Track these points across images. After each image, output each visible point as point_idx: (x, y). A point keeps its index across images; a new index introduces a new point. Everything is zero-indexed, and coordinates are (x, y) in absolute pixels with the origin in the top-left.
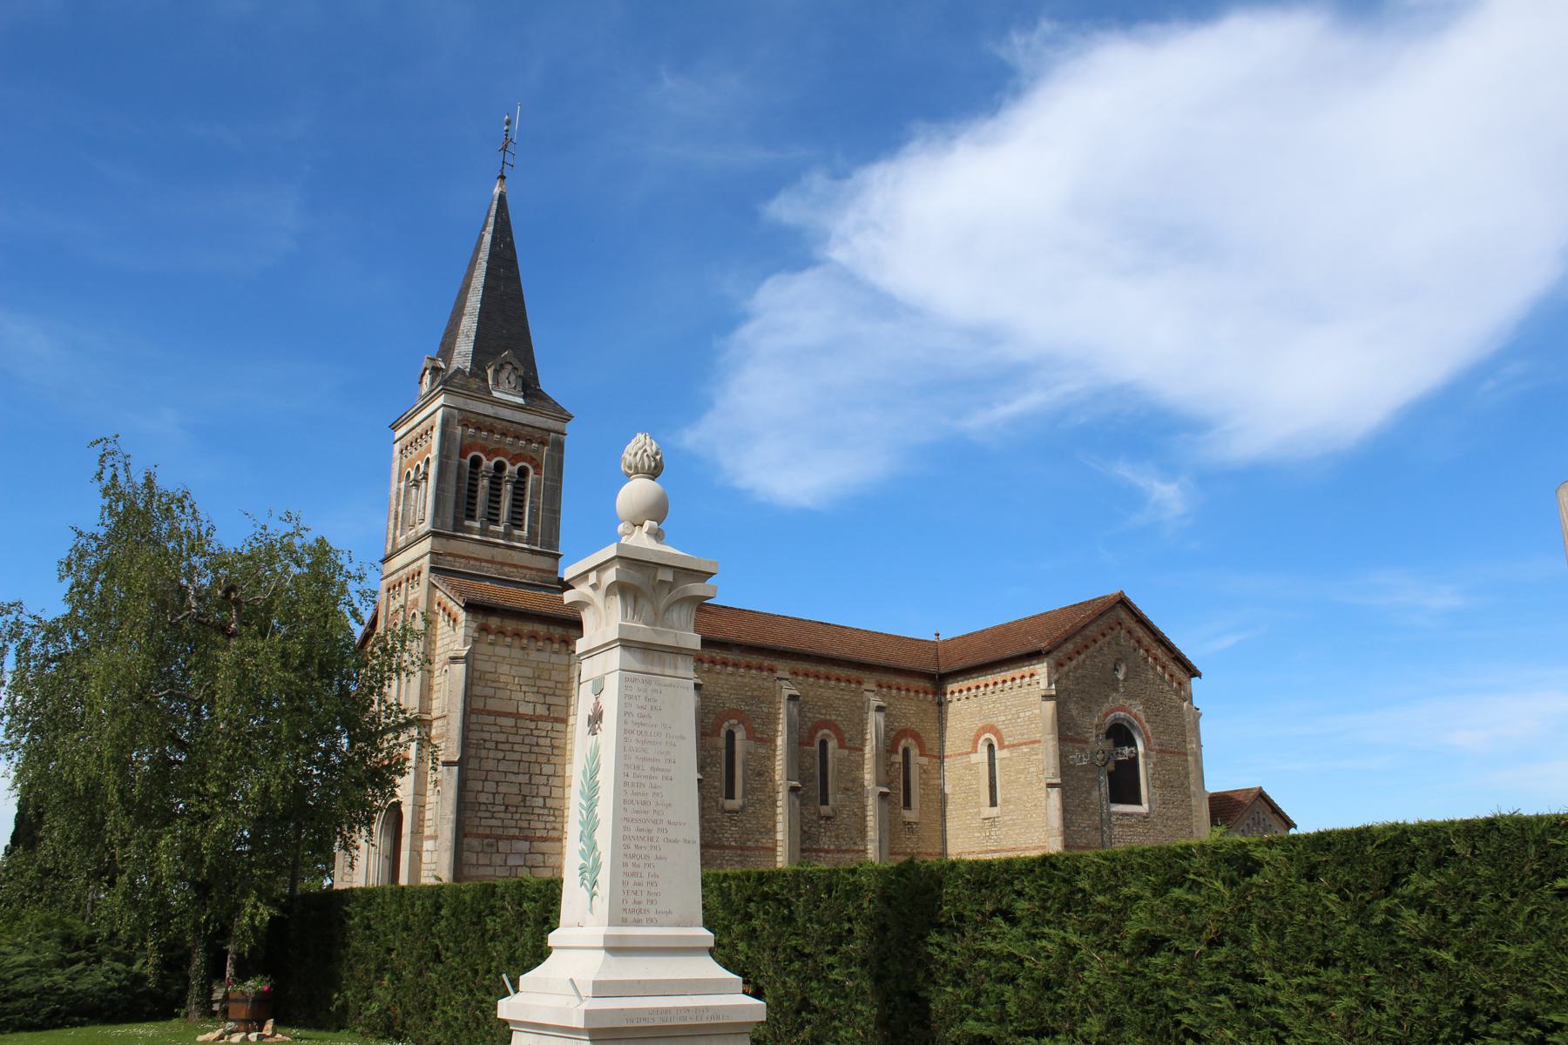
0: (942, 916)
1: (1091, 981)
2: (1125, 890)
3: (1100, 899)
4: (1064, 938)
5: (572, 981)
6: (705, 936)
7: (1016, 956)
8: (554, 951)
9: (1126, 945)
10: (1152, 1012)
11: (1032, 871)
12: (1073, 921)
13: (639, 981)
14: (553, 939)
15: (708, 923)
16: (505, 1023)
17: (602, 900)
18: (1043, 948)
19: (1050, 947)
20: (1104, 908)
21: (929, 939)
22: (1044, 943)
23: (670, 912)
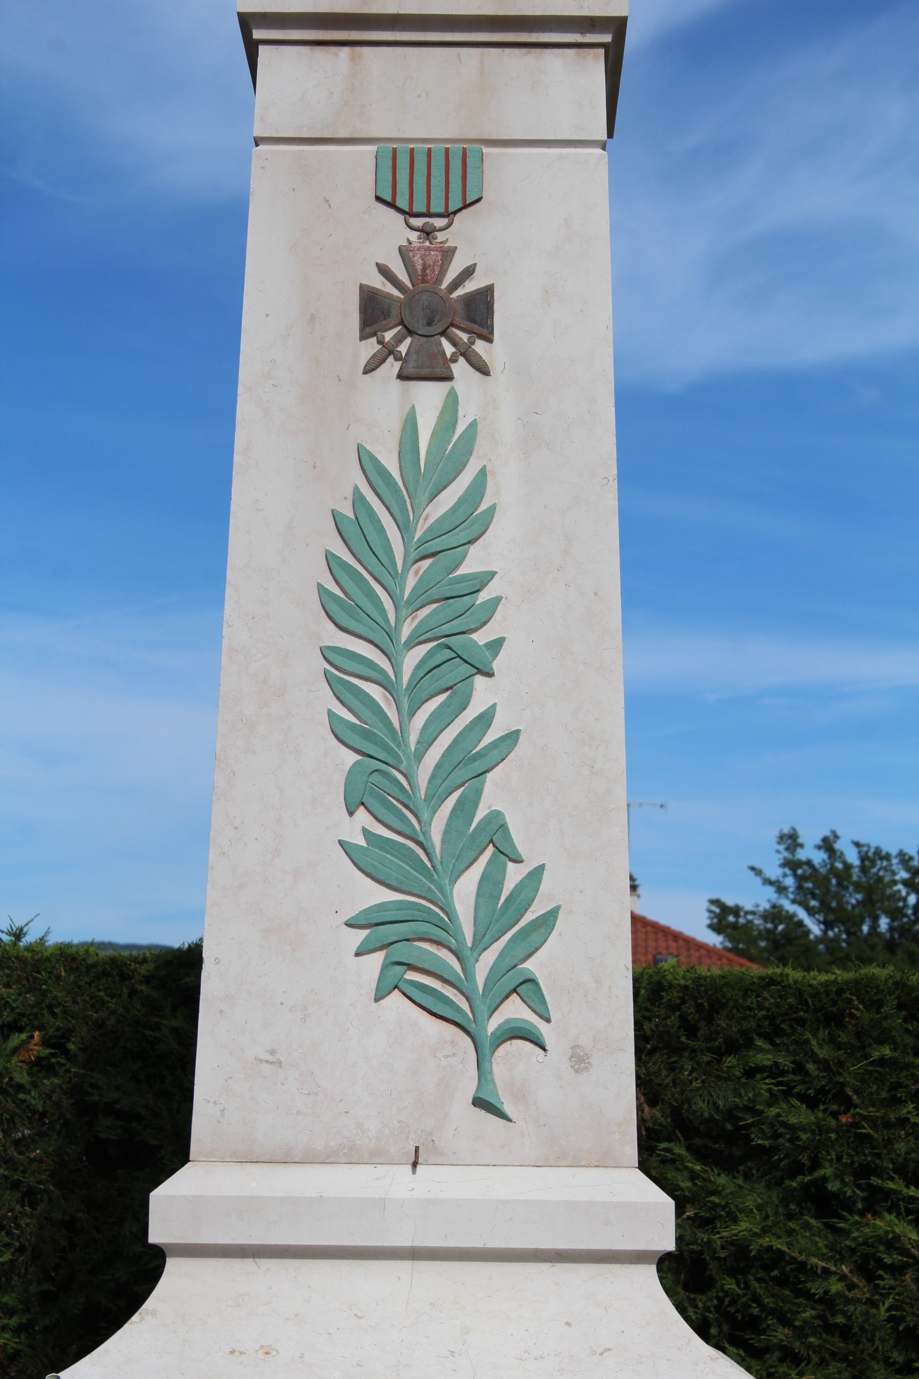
8: (172, 1265)
18: (892, 1243)
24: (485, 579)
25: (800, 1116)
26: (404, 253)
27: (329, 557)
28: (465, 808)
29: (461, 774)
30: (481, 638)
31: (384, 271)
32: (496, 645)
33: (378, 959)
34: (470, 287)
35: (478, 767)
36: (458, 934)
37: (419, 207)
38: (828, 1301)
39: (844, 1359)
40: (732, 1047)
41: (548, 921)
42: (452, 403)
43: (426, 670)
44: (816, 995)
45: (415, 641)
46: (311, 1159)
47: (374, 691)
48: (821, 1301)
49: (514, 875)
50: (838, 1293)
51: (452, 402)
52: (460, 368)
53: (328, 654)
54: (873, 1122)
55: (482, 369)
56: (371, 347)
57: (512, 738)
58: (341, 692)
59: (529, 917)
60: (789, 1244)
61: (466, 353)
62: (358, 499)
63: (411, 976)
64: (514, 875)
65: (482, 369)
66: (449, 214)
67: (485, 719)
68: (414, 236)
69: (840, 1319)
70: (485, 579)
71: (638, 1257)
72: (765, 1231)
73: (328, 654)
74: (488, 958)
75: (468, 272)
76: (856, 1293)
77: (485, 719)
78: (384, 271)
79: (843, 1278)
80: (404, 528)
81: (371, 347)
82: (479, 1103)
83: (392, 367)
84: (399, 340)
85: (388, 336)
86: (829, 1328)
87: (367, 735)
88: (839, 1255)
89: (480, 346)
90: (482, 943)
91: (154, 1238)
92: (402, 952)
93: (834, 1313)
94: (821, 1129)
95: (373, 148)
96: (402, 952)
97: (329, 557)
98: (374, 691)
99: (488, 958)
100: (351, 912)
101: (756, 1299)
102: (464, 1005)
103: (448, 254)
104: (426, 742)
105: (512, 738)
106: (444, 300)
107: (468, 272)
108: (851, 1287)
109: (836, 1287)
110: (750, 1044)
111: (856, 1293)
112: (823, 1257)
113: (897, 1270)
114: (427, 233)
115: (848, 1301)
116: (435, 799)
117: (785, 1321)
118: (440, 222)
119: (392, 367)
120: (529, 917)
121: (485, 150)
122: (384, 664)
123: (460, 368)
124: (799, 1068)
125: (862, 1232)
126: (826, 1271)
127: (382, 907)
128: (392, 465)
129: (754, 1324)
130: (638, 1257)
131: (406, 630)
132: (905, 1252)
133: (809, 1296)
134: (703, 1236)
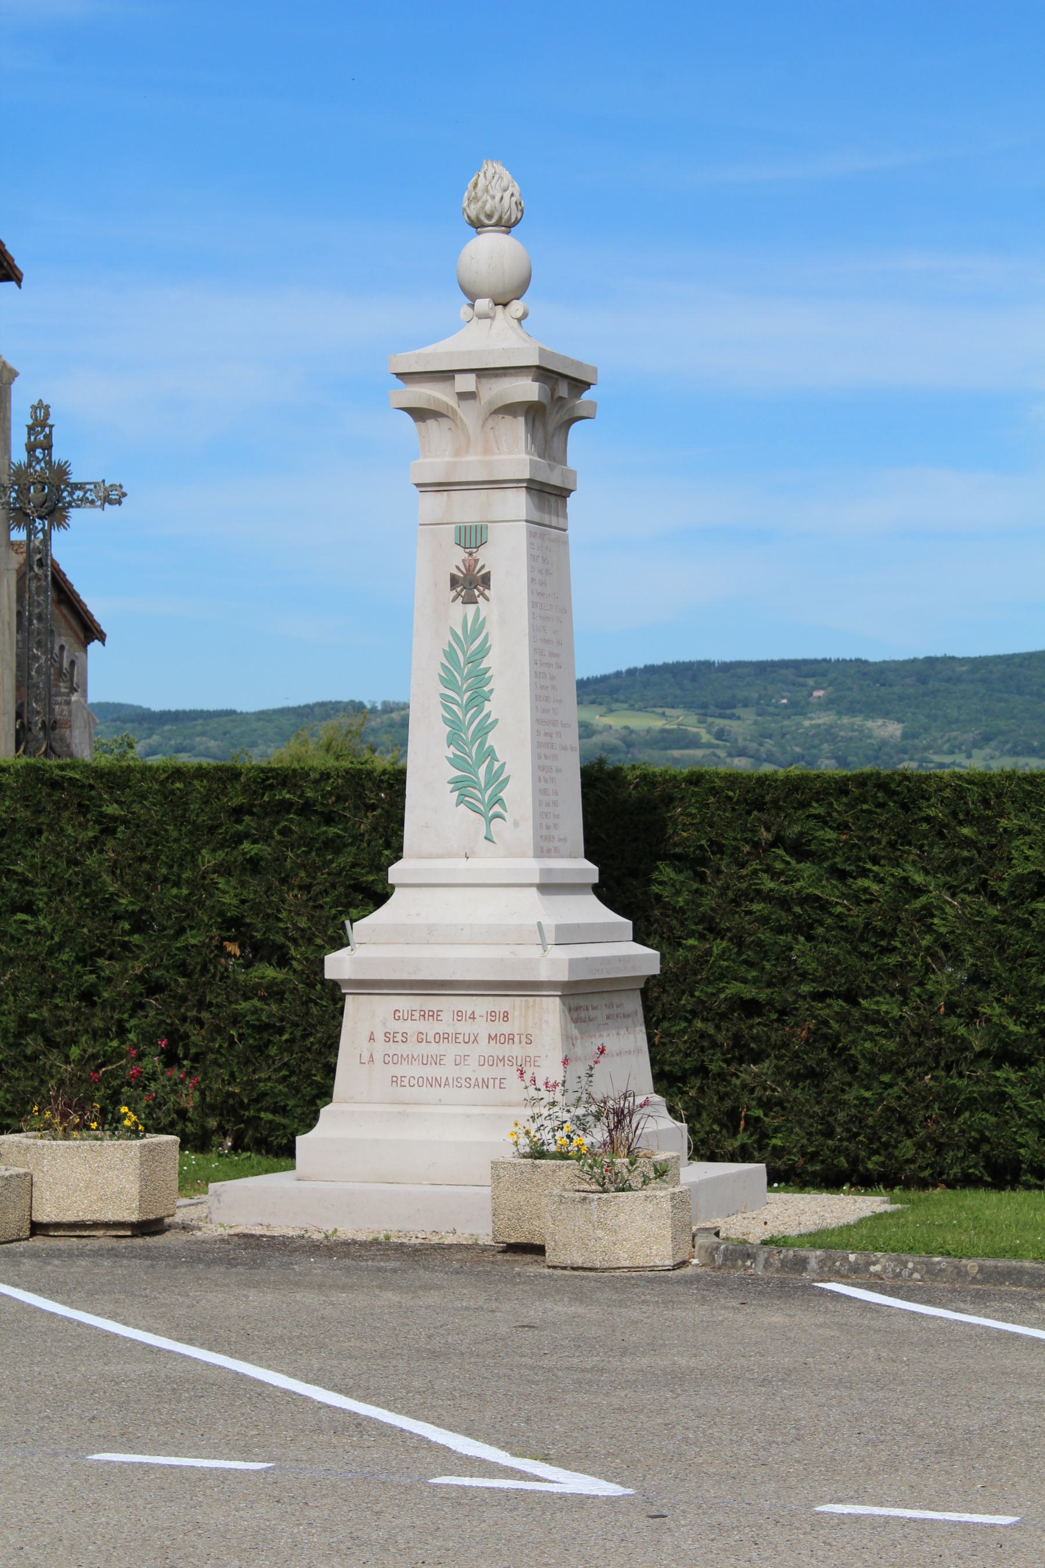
0: (675, 845)
1: (943, 930)
2: (1004, 822)
3: (966, 831)
4: (905, 879)
5: (539, 924)
6: (590, 871)
7: (818, 898)
8: (396, 889)
9: (1003, 889)
10: (1033, 965)
11: (846, 792)
12: (911, 857)
13: (578, 925)
14: (396, 873)
15: (590, 855)
16: (335, 984)
17: (516, 824)
18: (866, 890)
19: (875, 887)
20: (967, 843)
21: (655, 875)
22: (866, 883)
23: (565, 840)
24: (488, 669)
25: (832, 835)
26: (464, 561)
27: (442, 664)
28: (482, 745)
29: (480, 734)
30: (486, 689)
31: (457, 567)
32: (491, 691)
33: (457, 793)
34: (484, 572)
35: (486, 731)
36: (479, 784)
37: (468, 545)
38: (840, 917)
39: (846, 940)
40: (804, 805)
41: (506, 780)
42: (478, 610)
43: (471, 700)
44: (836, 783)
45: (467, 690)
46: (430, 857)
47: (454, 707)
48: (837, 916)
49: (497, 765)
50: (841, 912)
51: (478, 610)
52: (480, 599)
53: (443, 696)
54: (860, 838)
55: (487, 599)
56: (454, 593)
57: (496, 721)
58: (447, 708)
59: (501, 779)
60: (822, 892)
61: (482, 594)
62: (450, 645)
63: (466, 799)
64: (497, 765)
65: (487, 599)
66: (477, 548)
67: (488, 715)
68: (466, 555)
69: (844, 924)
70: (488, 669)
71: (531, 885)
72: (810, 886)
73: (443, 696)
74: (489, 792)
75: (483, 567)
76: (852, 913)
77: (488, 715)
78: (457, 567)
79: (845, 906)
80: (464, 653)
81: (454, 593)
82: (486, 838)
83: (460, 599)
84: (462, 591)
85: (459, 589)
86: (842, 928)
87: (452, 722)
88: (844, 896)
89: (487, 592)
90: (487, 787)
91: (390, 882)
92: (463, 791)
93: (843, 921)
94: (838, 841)
95: (454, 526)
96: (463, 791)
97: (442, 664)
98: (454, 707)
99: (489, 792)
100: (449, 779)
101: (809, 916)
102: (482, 808)
103: (476, 561)
104: (470, 723)
105: (496, 721)
106: (475, 576)
107: (483, 567)
108: (849, 910)
109: (839, 909)
110: (809, 805)
111: (852, 913)
112: (837, 897)
113: (869, 902)
114: (470, 554)
115: (849, 916)
116: (473, 742)
117: (822, 925)
118: (474, 550)
119: (460, 599)
120: (501, 779)
121: (489, 525)
122: (458, 698)
123: (480, 599)
124: (829, 814)
125: (850, 887)
126: (837, 903)
127: (457, 777)
128: (460, 633)
129: (811, 927)
130: (531, 885)
131: (465, 686)
132: (872, 894)
133: (831, 914)
134: (786, 888)
